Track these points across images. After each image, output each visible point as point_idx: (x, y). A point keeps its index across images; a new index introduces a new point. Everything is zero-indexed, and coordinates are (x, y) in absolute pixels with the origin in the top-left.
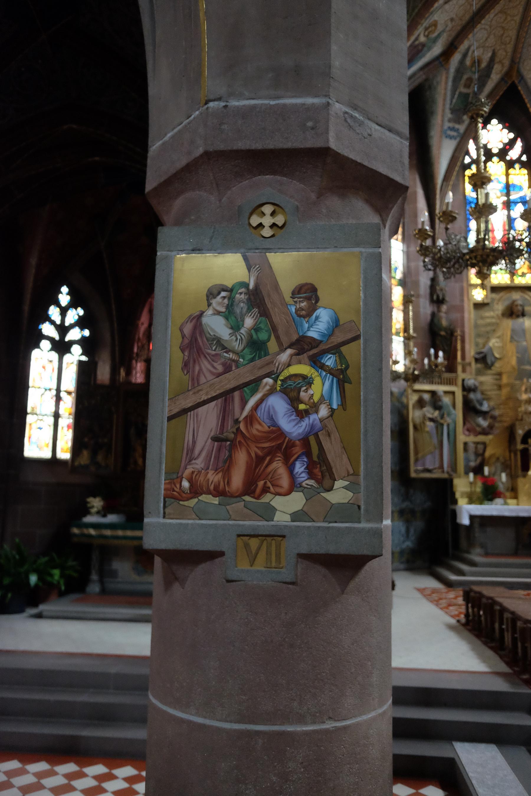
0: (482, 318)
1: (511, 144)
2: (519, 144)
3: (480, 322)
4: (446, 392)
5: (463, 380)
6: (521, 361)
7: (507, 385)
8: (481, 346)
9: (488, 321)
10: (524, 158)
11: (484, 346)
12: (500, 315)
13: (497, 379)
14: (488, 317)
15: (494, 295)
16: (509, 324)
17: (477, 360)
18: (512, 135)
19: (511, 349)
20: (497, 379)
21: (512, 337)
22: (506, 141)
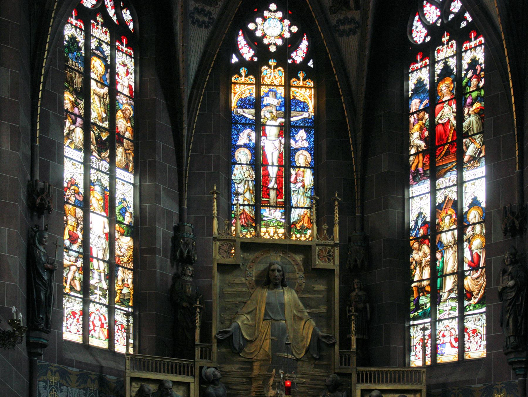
0: (230, 285)
1: (292, 43)
2: (304, 44)
3: (227, 289)
4: (174, 383)
5: (201, 368)
6: (276, 345)
7: (258, 377)
8: (228, 323)
9: (240, 289)
10: (311, 64)
11: (231, 323)
12: (253, 282)
13: (245, 369)
14: (238, 284)
15: (247, 255)
16: (264, 295)
17: (219, 342)
18: (295, 29)
19: (265, 328)
20: (245, 369)
21: (266, 314)
22: (287, 35)
